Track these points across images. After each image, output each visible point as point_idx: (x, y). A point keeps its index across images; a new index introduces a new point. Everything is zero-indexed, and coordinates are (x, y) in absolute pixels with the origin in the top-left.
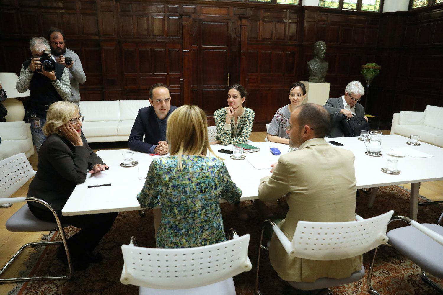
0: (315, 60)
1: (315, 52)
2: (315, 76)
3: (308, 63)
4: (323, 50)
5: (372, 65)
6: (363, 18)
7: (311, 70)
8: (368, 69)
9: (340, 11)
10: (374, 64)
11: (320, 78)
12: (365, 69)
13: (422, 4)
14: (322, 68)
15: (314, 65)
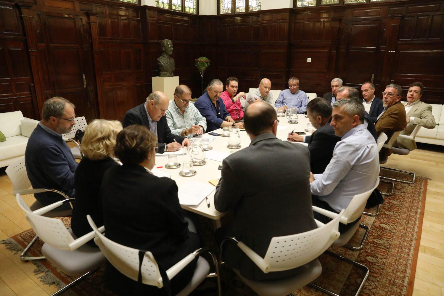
0: (164, 56)
1: (163, 49)
2: (166, 71)
3: (158, 59)
4: (171, 47)
5: (204, 59)
6: (185, 19)
7: (162, 66)
8: (202, 62)
9: (170, 12)
10: (205, 58)
11: (171, 72)
12: (199, 62)
13: (227, 11)
14: (171, 64)
15: (164, 61)
